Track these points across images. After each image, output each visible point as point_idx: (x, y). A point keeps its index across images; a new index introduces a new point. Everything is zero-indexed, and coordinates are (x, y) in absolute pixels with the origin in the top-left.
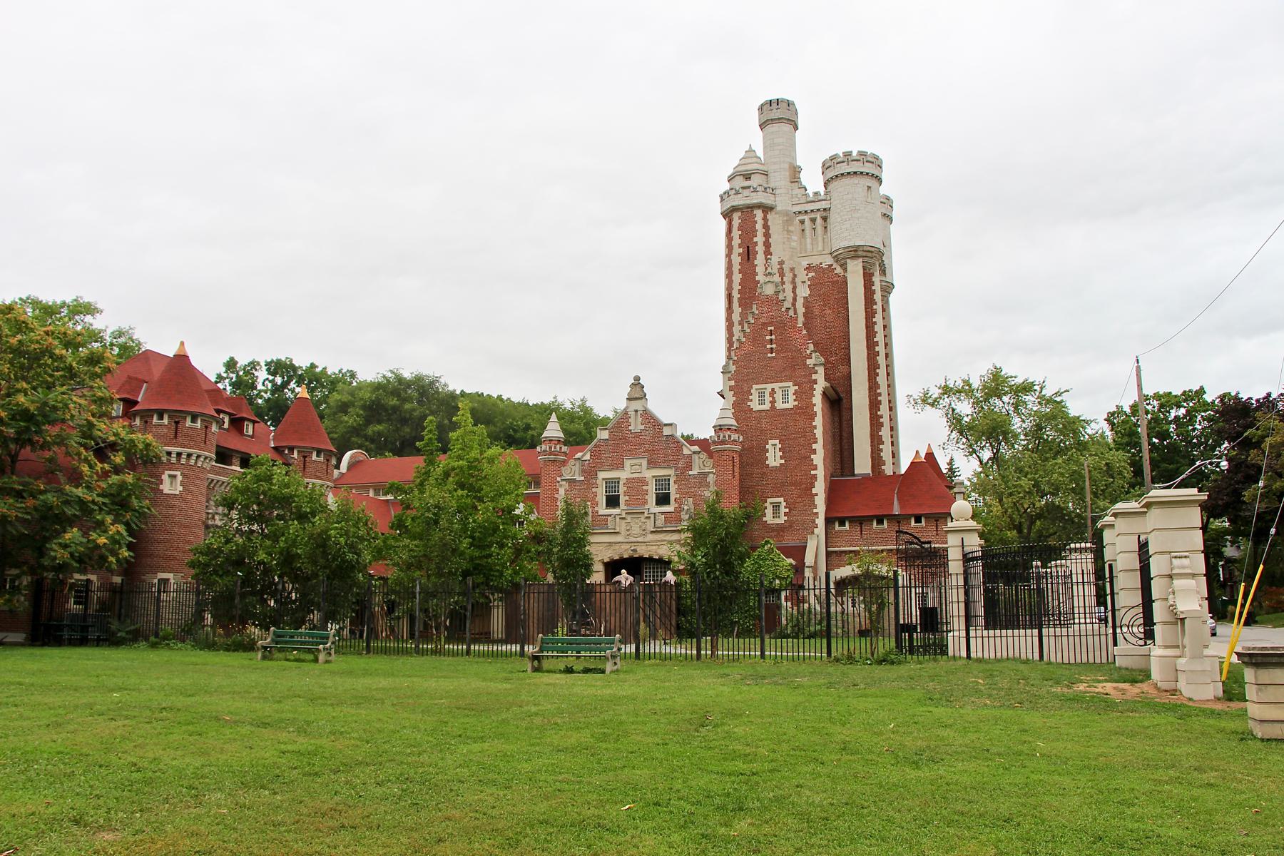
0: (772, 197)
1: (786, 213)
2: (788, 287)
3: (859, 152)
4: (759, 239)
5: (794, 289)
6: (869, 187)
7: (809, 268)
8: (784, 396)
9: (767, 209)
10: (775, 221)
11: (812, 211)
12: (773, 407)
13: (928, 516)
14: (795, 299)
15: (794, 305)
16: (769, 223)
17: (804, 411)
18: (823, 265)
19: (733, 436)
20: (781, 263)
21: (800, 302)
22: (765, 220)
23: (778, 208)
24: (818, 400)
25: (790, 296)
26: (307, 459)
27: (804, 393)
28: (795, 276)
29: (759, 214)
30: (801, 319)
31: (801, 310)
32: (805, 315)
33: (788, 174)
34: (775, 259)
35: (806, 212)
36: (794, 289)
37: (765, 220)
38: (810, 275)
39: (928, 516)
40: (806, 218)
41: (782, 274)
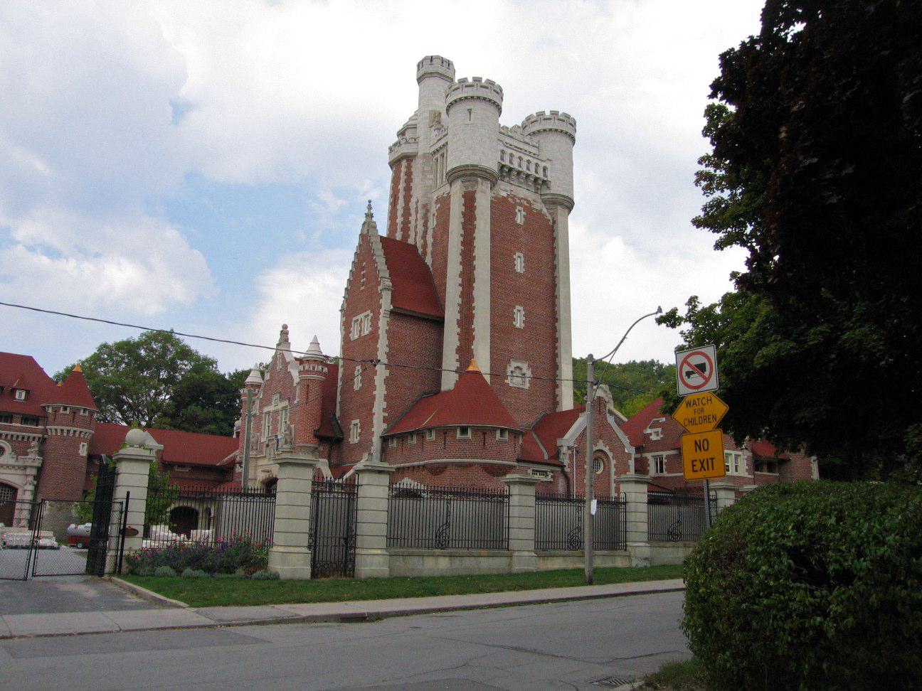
0: (415, 146)
1: (424, 156)
2: (420, 222)
3: (473, 78)
4: (402, 186)
5: (425, 225)
6: (470, 111)
7: (436, 202)
8: (363, 326)
9: (410, 158)
10: (417, 166)
11: (441, 148)
12: (360, 335)
13: (511, 432)
14: (425, 232)
15: (424, 237)
16: (413, 170)
17: (374, 336)
18: (445, 195)
19: (316, 367)
20: (417, 202)
21: (430, 232)
22: (409, 167)
23: (420, 153)
24: (383, 323)
25: (420, 229)
26: (76, 415)
27: (375, 321)
28: (428, 211)
29: (404, 163)
30: (429, 250)
31: (430, 240)
32: (433, 245)
33: (428, 121)
34: (413, 200)
35: (438, 150)
36: (425, 225)
37: (409, 167)
38: (439, 205)
39: (511, 432)
40: (438, 155)
41: (417, 212)
